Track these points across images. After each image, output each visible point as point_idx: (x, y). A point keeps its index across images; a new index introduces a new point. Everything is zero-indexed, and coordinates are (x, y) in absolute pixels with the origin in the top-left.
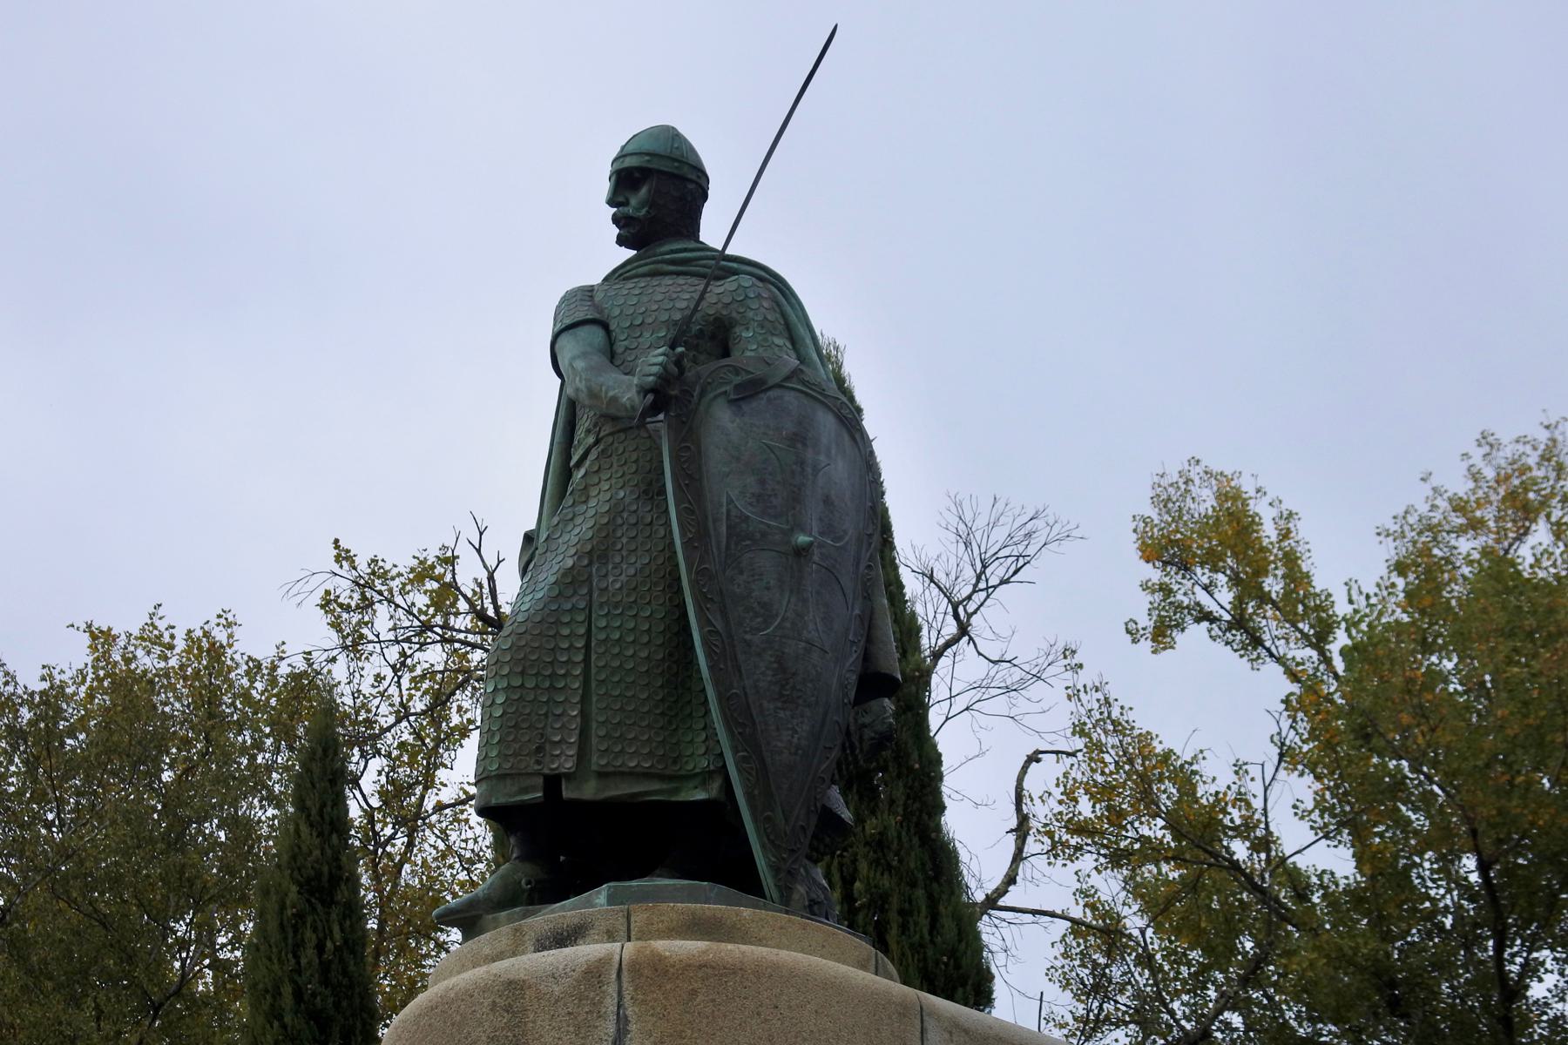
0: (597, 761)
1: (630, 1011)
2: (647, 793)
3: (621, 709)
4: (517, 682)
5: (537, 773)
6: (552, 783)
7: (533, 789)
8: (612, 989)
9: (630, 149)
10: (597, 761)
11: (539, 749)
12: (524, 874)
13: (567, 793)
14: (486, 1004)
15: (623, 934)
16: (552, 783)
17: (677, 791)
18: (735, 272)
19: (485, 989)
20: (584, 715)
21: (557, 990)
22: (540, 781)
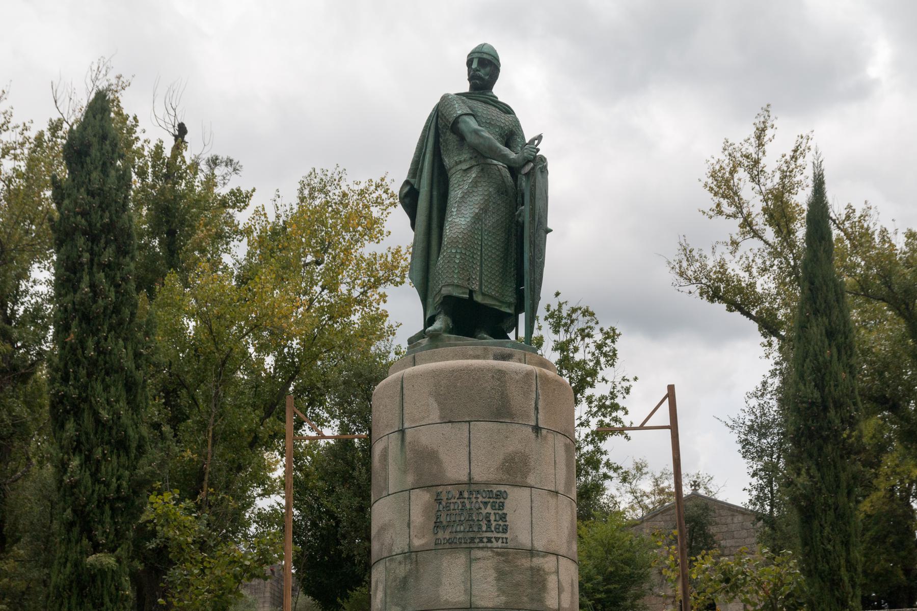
0: (485, 289)
1: (540, 391)
2: (495, 305)
3: (491, 272)
5: (468, 288)
6: (471, 292)
7: (464, 293)
8: (534, 382)
9: (477, 50)
11: (469, 279)
14: (490, 375)
15: (523, 361)
16: (471, 292)
17: (501, 307)
18: (510, 113)
19: (489, 370)
20: (481, 270)
22: (468, 291)
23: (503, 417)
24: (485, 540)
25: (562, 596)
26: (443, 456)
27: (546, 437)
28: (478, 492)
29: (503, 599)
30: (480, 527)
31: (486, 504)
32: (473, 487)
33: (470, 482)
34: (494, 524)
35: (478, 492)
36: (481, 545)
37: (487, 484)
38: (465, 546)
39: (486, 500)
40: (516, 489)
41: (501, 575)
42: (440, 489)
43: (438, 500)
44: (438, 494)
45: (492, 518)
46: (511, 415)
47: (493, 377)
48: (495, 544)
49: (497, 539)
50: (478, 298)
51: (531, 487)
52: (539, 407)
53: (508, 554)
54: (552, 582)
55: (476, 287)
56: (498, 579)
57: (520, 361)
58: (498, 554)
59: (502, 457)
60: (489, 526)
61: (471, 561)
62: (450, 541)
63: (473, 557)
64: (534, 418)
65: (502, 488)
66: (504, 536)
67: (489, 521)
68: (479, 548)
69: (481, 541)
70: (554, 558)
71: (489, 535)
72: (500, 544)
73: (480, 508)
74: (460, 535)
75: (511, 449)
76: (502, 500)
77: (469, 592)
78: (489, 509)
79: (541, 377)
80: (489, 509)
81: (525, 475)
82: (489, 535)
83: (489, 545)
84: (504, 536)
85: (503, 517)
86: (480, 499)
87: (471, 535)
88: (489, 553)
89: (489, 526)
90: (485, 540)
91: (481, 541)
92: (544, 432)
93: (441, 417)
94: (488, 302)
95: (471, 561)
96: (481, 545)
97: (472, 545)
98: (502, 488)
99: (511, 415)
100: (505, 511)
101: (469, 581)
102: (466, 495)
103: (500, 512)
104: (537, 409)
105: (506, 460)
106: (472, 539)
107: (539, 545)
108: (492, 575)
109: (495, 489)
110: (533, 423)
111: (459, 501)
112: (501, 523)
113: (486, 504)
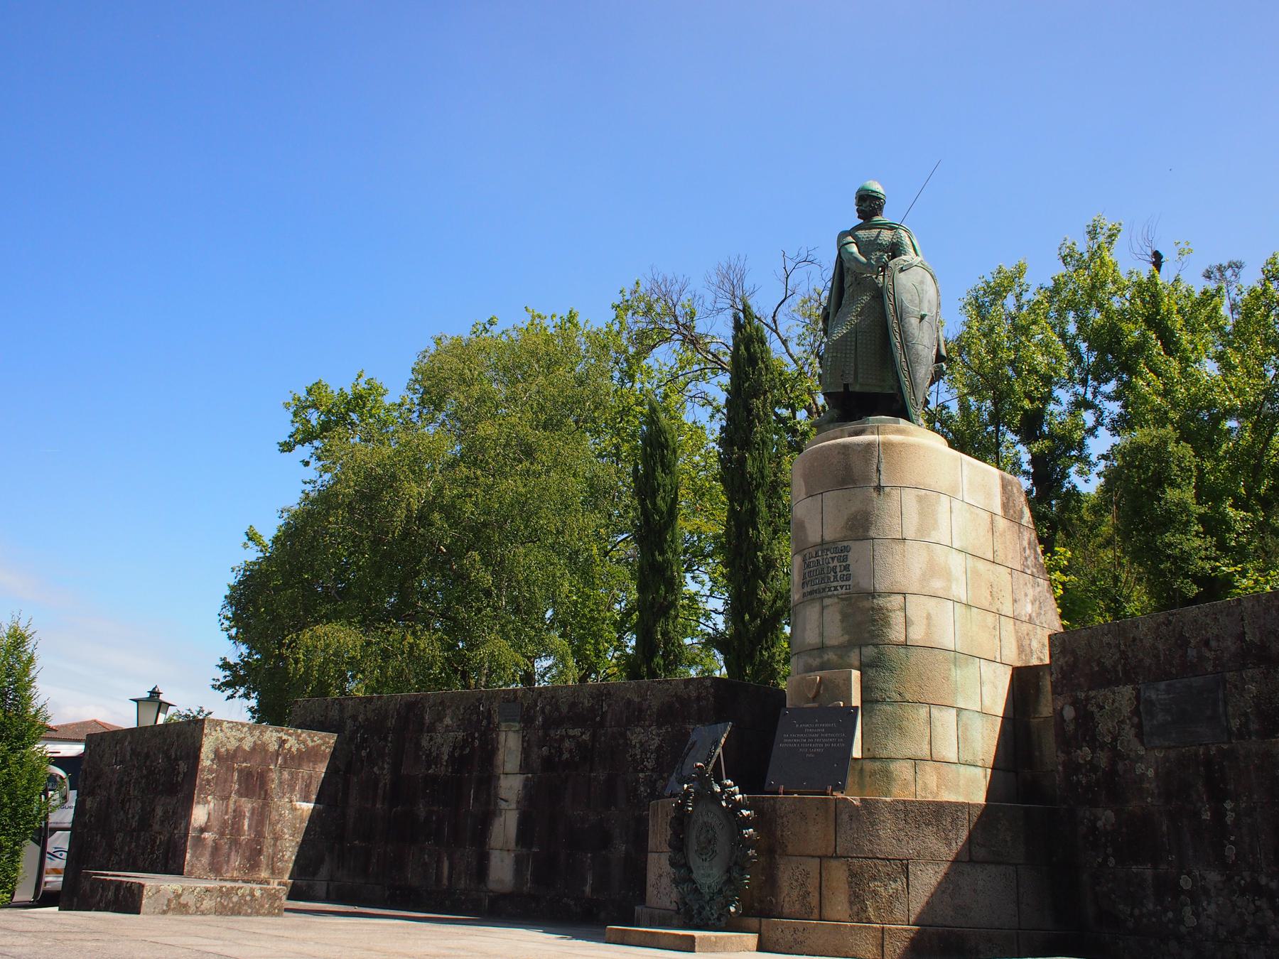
1: (882, 456)
4: (835, 354)
6: (846, 386)
10: (860, 380)
12: (835, 413)
13: (850, 390)
15: (876, 433)
16: (846, 386)
21: (859, 449)
23: (847, 484)
24: (832, 589)
25: (911, 630)
26: (808, 526)
27: (889, 495)
28: (827, 550)
29: (846, 637)
30: (829, 578)
31: (833, 559)
32: (824, 546)
33: (823, 542)
34: (839, 574)
35: (827, 550)
36: (830, 593)
37: (834, 542)
38: (818, 596)
39: (834, 555)
40: (858, 543)
41: (845, 617)
42: (805, 552)
43: (804, 560)
44: (805, 556)
45: (838, 570)
46: (854, 482)
47: (839, 453)
48: (840, 591)
49: (842, 587)
50: (856, 388)
51: (873, 539)
52: (881, 469)
53: (850, 598)
54: (897, 619)
55: (851, 380)
56: (842, 621)
57: (873, 433)
58: (842, 599)
59: (845, 518)
60: (835, 577)
61: (823, 608)
62: (811, 593)
63: (824, 604)
64: (877, 481)
65: (845, 544)
66: (847, 583)
67: (835, 573)
68: (829, 597)
69: (830, 588)
70: (900, 597)
71: (835, 584)
72: (844, 591)
73: (829, 563)
74: (816, 587)
75: (853, 509)
76: (846, 553)
77: (822, 634)
78: (836, 563)
79: (884, 444)
80: (836, 563)
81: (867, 529)
82: (835, 584)
83: (835, 593)
84: (847, 583)
85: (847, 568)
86: (830, 555)
87: (823, 586)
88: (836, 600)
89: (835, 577)
90: (832, 589)
91: (830, 590)
92: (887, 489)
93: (806, 494)
94: (867, 389)
95: (823, 608)
96: (830, 593)
97: (824, 594)
98: (845, 544)
99: (854, 482)
100: (848, 563)
101: (822, 625)
102: (820, 553)
103: (844, 564)
104: (878, 471)
105: (849, 520)
106: (824, 589)
107: (881, 587)
108: (838, 617)
109: (840, 545)
110: (876, 485)
111: (815, 559)
112: (845, 573)
113: (833, 559)
